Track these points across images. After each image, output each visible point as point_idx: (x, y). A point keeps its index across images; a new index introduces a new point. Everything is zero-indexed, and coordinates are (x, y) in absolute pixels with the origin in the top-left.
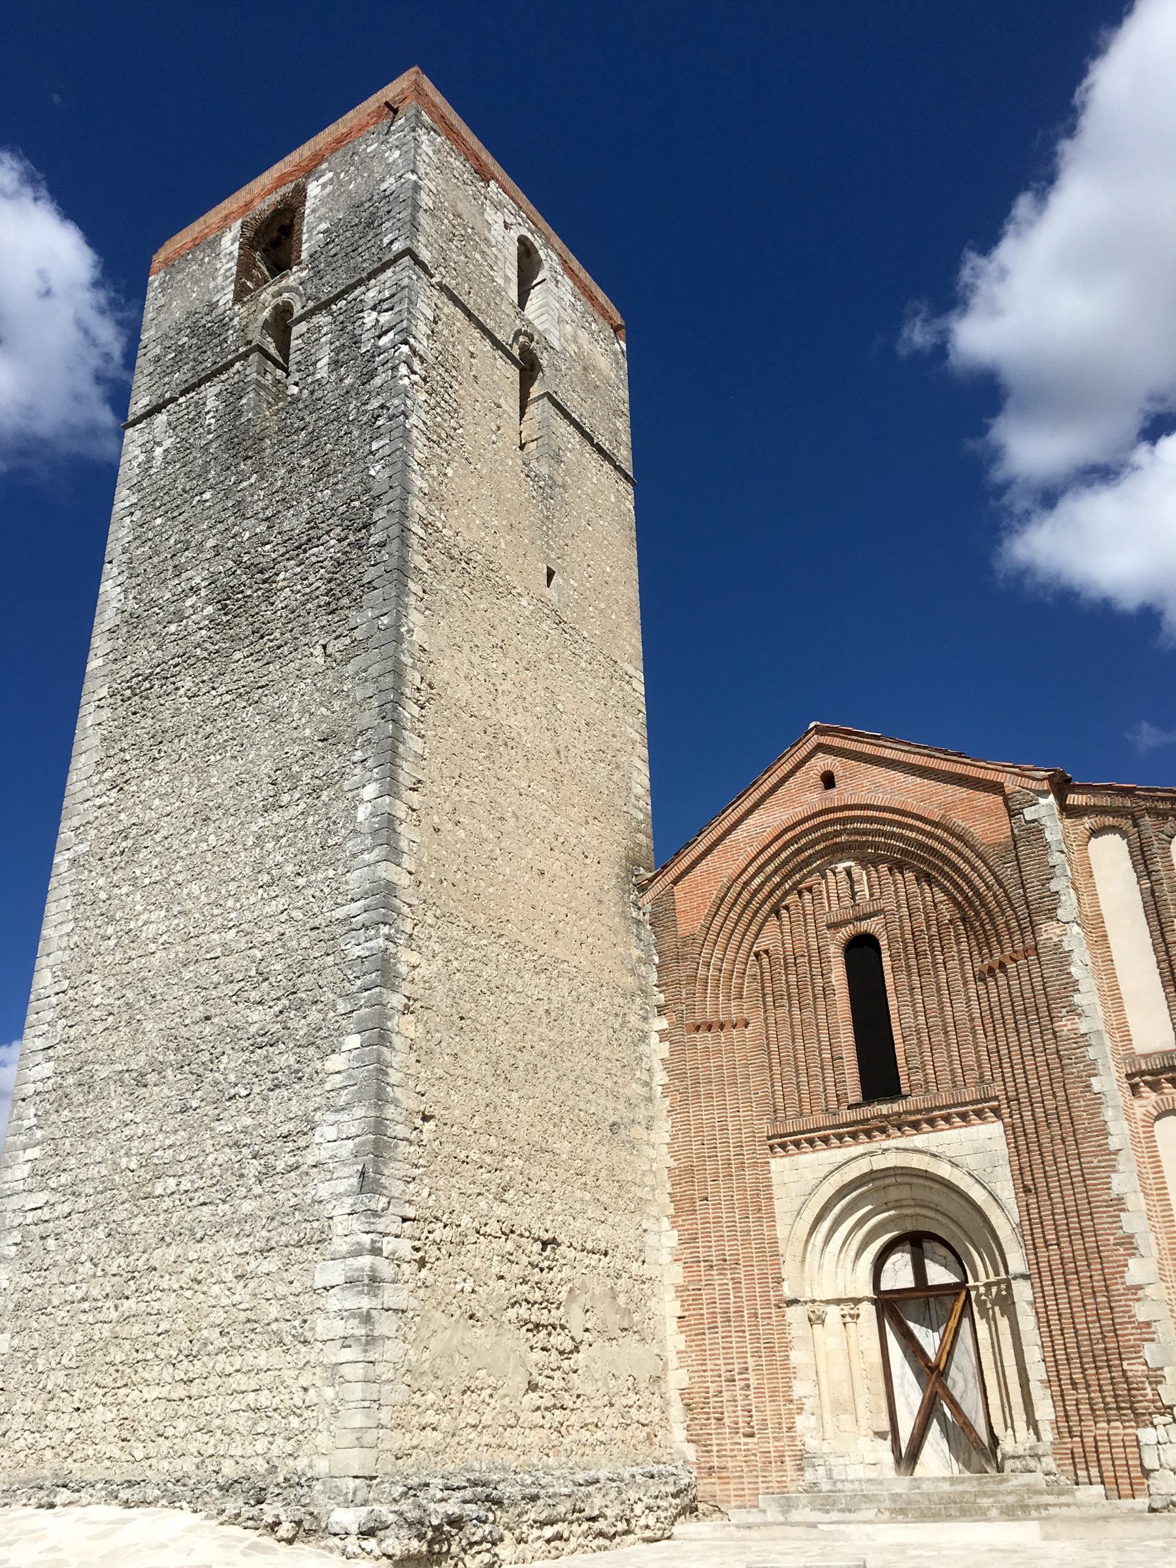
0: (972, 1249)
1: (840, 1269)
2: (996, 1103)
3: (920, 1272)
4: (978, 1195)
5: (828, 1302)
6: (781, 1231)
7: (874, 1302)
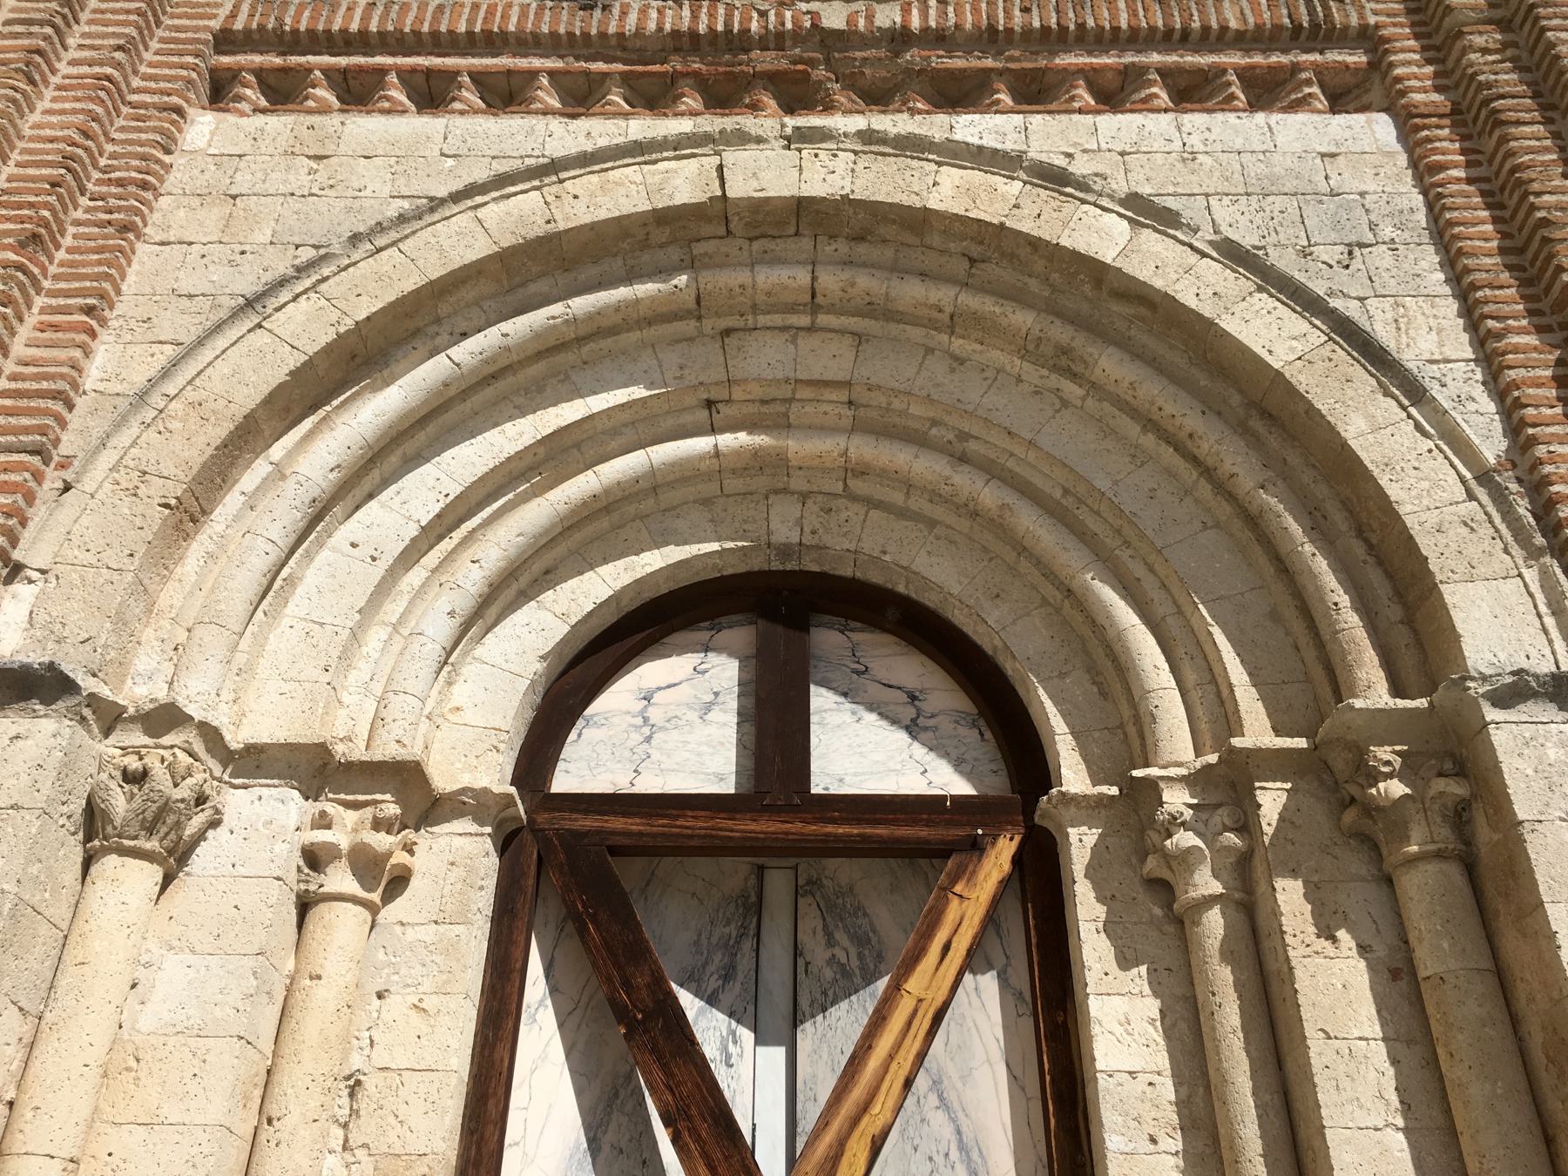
0: (1125, 616)
1: (376, 636)
2: (1357, 58)
3: (776, 732)
4: (1270, 333)
5: (253, 762)
6: (112, 364)
7: (507, 843)
